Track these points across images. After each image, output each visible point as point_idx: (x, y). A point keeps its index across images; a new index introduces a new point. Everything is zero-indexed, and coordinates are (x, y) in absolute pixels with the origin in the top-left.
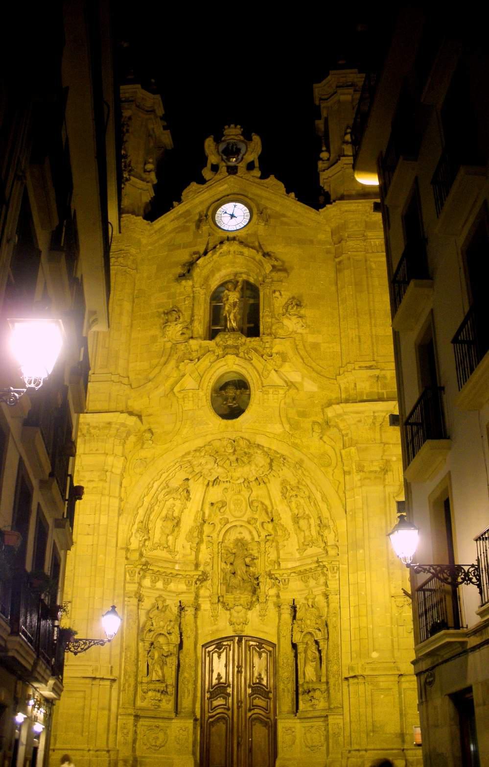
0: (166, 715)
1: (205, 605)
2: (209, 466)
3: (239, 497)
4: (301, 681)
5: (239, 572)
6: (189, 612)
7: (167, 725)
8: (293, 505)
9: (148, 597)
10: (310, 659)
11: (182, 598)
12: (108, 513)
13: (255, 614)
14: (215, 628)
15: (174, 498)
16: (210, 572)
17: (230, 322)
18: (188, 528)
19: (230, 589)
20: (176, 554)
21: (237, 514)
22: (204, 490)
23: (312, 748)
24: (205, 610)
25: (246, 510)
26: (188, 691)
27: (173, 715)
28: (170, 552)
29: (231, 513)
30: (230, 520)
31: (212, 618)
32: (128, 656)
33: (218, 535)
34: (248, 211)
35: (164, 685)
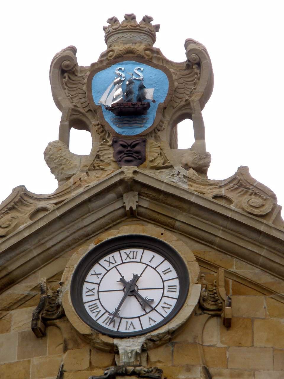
34: (173, 274)
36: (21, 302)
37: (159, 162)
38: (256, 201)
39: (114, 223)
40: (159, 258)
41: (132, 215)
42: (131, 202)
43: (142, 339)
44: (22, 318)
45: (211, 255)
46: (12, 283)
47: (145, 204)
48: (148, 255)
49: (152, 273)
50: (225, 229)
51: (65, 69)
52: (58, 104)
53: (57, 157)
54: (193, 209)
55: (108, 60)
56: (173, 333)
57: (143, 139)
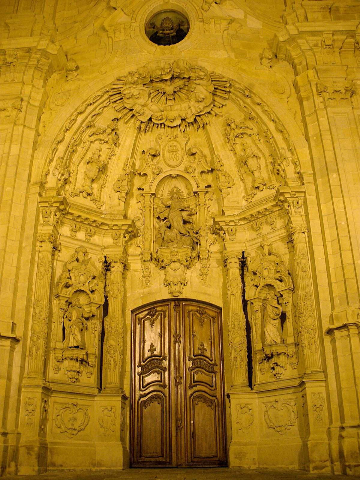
0: (86, 391)
1: (135, 265)
2: (142, 101)
3: (175, 143)
5: (175, 225)
6: (117, 269)
7: (87, 403)
8: (238, 148)
9: (66, 247)
10: (272, 315)
11: (107, 252)
12: (21, 142)
13: (195, 274)
14: (146, 290)
16: (142, 228)
18: (116, 177)
19: (163, 242)
20: (102, 204)
21: (172, 163)
22: (135, 135)
23: (278, 429)
24: (136, 270)
25: (183, 158)
26: (115, 361)
27: (96, 391)
29: (165, 162)
30: (164, 170)
31: (144, 279)
32: (37, 312)
33: (150, 186)
35: (84, 352)
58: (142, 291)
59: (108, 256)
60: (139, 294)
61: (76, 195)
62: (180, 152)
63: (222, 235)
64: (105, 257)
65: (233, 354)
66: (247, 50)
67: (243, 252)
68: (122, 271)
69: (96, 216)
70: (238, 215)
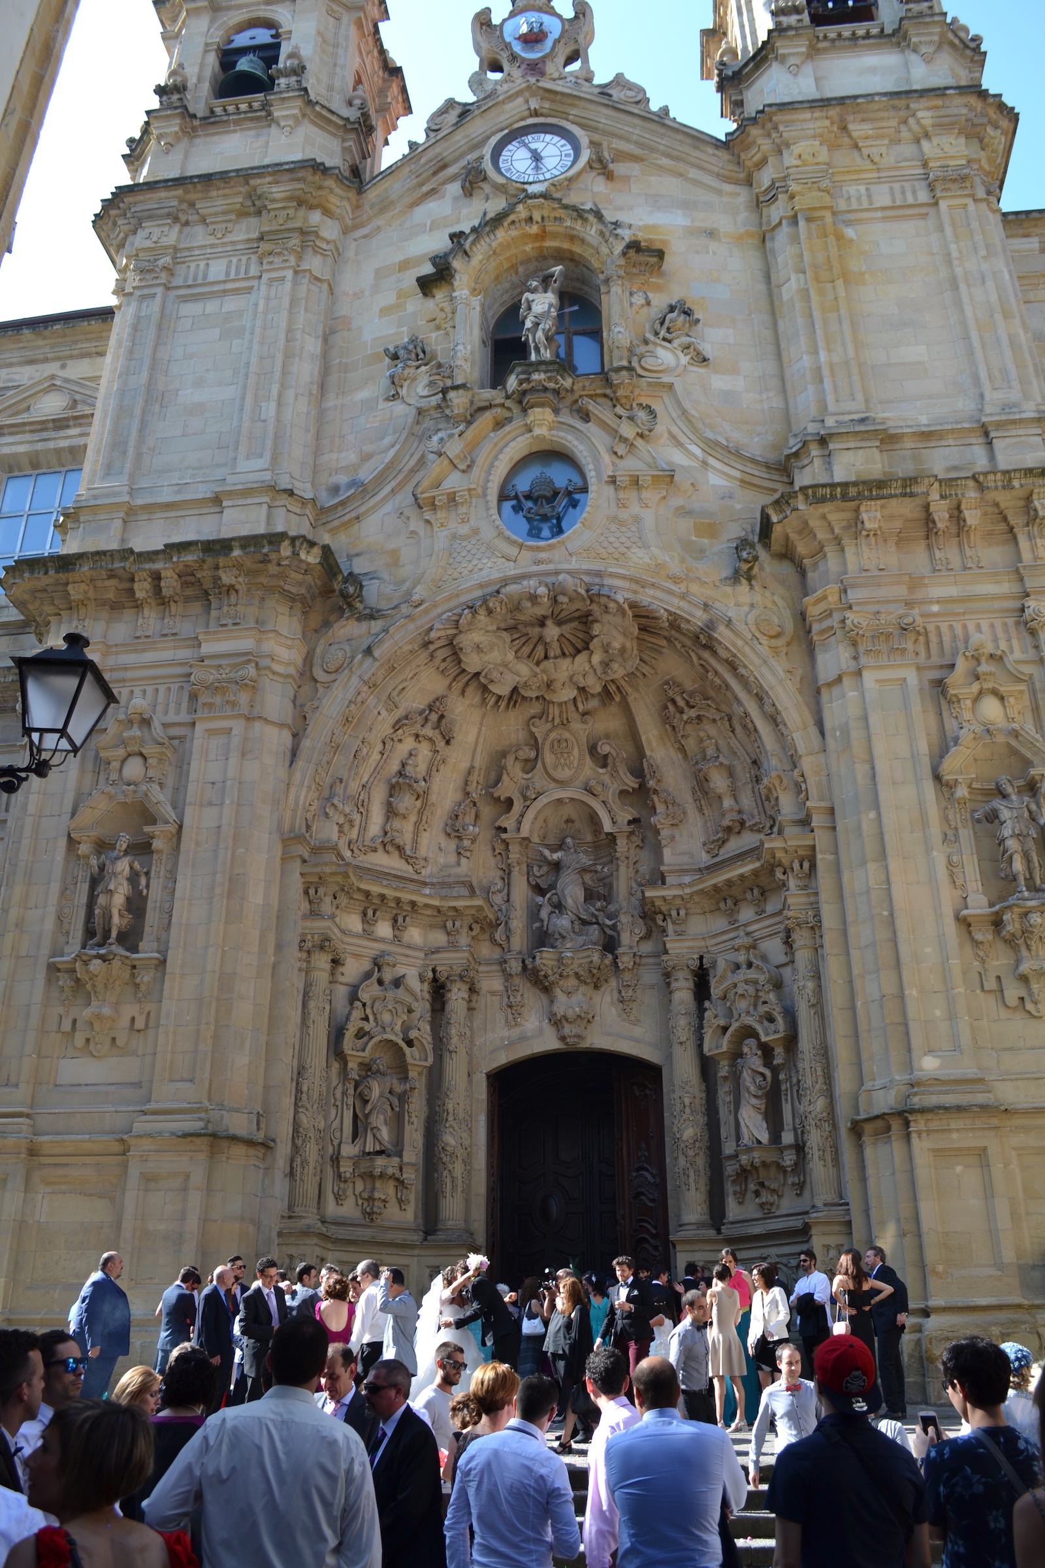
0: (399, 1237)
1: (491, 983)
2: (495, 656)
3: (567, 735)
4: (728, 1148)
5: (570, 902)
6: (457, 996)
8: (691, 744)
9: (357, 956)
10: (752, 1088)
14: (515, 1032)
15: (417, 736)
17: (537, 349)
19: (542, 938)
24: (493, 993)
27: (416, 1238)
28: (408, 860)
32: (305, 1089)
34: (569, 147)
35: (395, 1161)
36: (453, 179)
37: (556, 75)
38: (630, 93)
39: (523, 119)
40: (556, 138)
41: (536, 113)
42: (534, 104)
43: (546, 184)
44: (455, 188)
45: (596, 137)
46: (445, 167)
47: (547, 105)
48: (548, 137)
49: (554, 153)
50: (607, 117)
51: (483, 21)
52: (478, 52)
53: (476, 82)
54: (582, 104)
55: (513, 14)
56: (570, 180)
57: (543, 59)
58: (506, 1033)
59: (439, 969)
60: (502, 1039)
61: (375, 850)
62: (576, 752)
63: (660, 923)
64: (434, 971)
65: (682, 1161)
66: (706, 541)
67: (701, 958)
68: (466, 996)
69: (413, 892)
70: (690, 885)
